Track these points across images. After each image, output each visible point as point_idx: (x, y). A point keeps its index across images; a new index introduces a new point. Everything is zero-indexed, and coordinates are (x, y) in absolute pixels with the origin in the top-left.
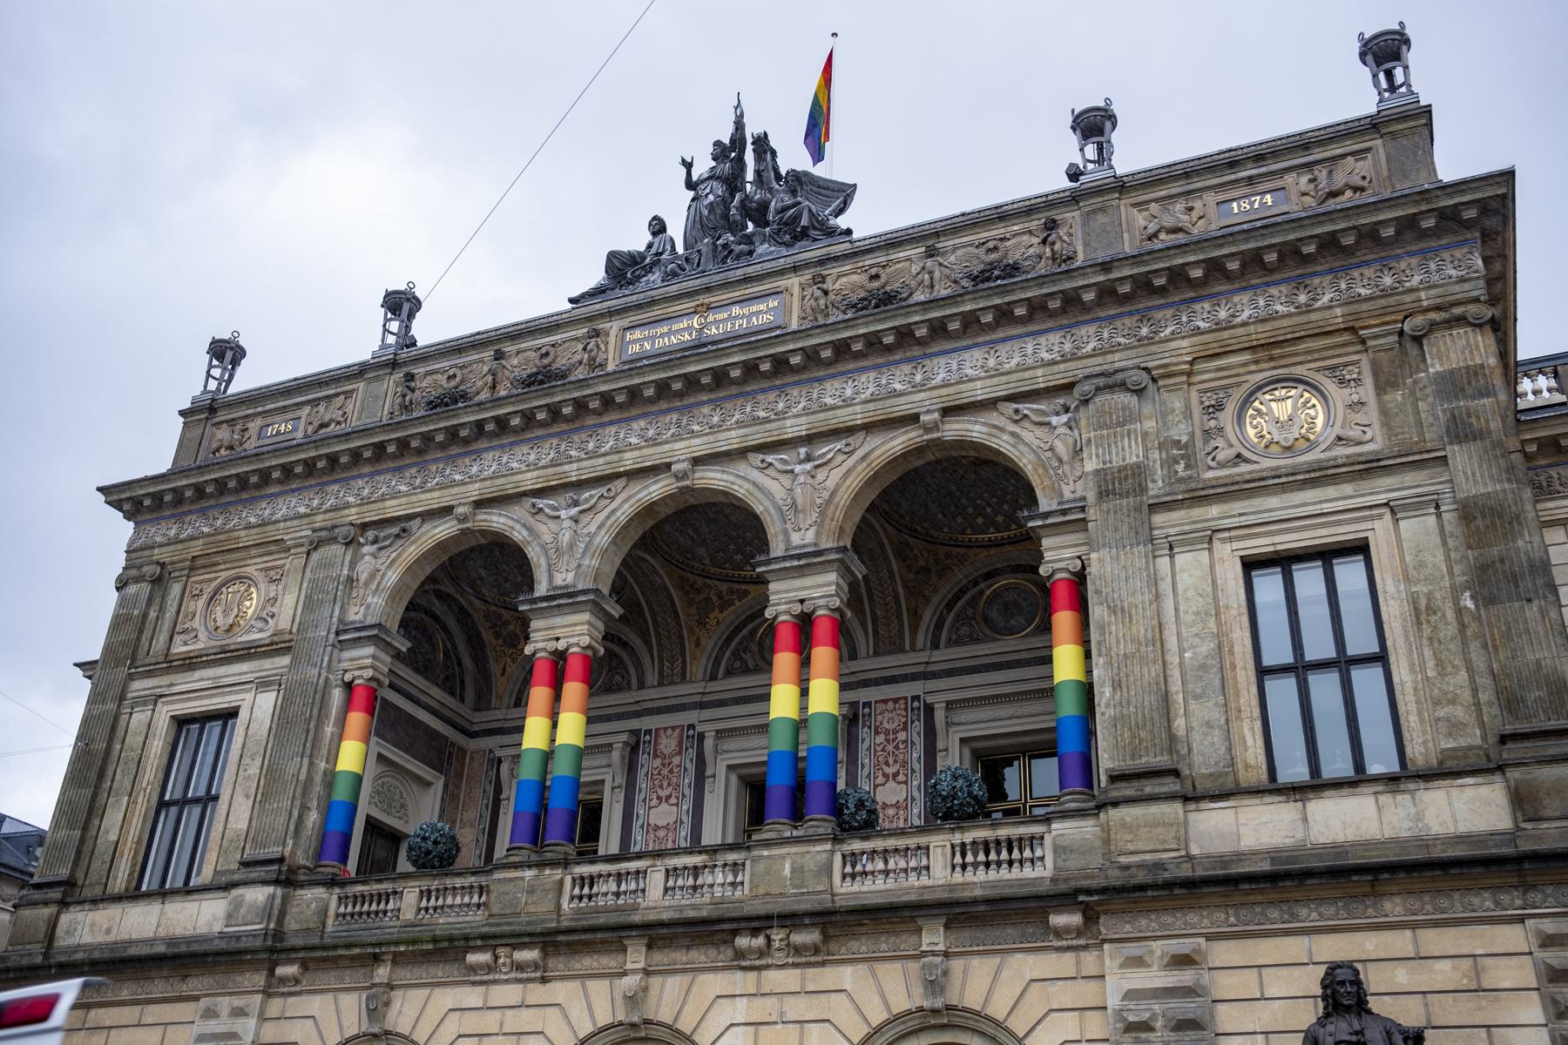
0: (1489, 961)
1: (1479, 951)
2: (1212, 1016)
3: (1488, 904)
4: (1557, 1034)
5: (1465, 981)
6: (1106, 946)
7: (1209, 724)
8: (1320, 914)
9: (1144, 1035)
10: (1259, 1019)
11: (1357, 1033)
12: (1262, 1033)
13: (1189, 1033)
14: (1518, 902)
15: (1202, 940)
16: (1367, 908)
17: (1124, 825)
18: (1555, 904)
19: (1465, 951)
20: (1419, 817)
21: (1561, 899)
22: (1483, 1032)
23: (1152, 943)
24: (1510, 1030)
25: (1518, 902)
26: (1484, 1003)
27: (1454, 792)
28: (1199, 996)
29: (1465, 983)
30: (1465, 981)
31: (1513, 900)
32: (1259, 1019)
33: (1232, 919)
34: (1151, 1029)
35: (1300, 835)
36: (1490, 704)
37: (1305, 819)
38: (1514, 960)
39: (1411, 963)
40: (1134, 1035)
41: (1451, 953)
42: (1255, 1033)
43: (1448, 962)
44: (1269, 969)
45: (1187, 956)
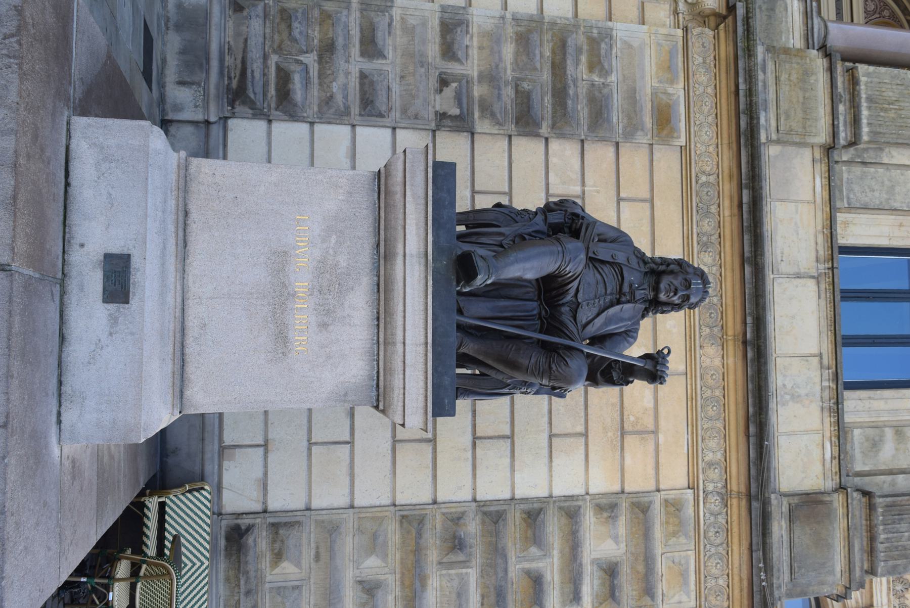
0: (651, 447)
2: (603, 140)
3: (709, 457)
4: (580, 503)
5: (632, 418)
6: (680, 32)
7: (891, 190)
9: (584, 58)
10: (598, 192)
11: (632, 293)
12: (583, 192)
13: (586, 111)
14: (710, 487)
15: (682, 141)
16: (711, 328)
17: (807, 73)
18: (708, 522)
19: (662, 423)
20: (795, 398)
22: (580, 428)
23: (681, 85)
24: (583, 457)
25: (710, 487)
26: (610, 434)
27: (818, 438)
28: (625, 128)
29: (630, 419)
30: (632, 418)
31: (712, 481)
32: (598, 192)
33: (704, 179)
34: (591, 69)
35: (784, 268)
36: (893, 484)
37: (798, 276)
38: (651, 472)
40: (585, 47)
41: (661, 409)
42: (583, 184)
43: (651, 405)
44: (648, 213)
45: (668, 121)
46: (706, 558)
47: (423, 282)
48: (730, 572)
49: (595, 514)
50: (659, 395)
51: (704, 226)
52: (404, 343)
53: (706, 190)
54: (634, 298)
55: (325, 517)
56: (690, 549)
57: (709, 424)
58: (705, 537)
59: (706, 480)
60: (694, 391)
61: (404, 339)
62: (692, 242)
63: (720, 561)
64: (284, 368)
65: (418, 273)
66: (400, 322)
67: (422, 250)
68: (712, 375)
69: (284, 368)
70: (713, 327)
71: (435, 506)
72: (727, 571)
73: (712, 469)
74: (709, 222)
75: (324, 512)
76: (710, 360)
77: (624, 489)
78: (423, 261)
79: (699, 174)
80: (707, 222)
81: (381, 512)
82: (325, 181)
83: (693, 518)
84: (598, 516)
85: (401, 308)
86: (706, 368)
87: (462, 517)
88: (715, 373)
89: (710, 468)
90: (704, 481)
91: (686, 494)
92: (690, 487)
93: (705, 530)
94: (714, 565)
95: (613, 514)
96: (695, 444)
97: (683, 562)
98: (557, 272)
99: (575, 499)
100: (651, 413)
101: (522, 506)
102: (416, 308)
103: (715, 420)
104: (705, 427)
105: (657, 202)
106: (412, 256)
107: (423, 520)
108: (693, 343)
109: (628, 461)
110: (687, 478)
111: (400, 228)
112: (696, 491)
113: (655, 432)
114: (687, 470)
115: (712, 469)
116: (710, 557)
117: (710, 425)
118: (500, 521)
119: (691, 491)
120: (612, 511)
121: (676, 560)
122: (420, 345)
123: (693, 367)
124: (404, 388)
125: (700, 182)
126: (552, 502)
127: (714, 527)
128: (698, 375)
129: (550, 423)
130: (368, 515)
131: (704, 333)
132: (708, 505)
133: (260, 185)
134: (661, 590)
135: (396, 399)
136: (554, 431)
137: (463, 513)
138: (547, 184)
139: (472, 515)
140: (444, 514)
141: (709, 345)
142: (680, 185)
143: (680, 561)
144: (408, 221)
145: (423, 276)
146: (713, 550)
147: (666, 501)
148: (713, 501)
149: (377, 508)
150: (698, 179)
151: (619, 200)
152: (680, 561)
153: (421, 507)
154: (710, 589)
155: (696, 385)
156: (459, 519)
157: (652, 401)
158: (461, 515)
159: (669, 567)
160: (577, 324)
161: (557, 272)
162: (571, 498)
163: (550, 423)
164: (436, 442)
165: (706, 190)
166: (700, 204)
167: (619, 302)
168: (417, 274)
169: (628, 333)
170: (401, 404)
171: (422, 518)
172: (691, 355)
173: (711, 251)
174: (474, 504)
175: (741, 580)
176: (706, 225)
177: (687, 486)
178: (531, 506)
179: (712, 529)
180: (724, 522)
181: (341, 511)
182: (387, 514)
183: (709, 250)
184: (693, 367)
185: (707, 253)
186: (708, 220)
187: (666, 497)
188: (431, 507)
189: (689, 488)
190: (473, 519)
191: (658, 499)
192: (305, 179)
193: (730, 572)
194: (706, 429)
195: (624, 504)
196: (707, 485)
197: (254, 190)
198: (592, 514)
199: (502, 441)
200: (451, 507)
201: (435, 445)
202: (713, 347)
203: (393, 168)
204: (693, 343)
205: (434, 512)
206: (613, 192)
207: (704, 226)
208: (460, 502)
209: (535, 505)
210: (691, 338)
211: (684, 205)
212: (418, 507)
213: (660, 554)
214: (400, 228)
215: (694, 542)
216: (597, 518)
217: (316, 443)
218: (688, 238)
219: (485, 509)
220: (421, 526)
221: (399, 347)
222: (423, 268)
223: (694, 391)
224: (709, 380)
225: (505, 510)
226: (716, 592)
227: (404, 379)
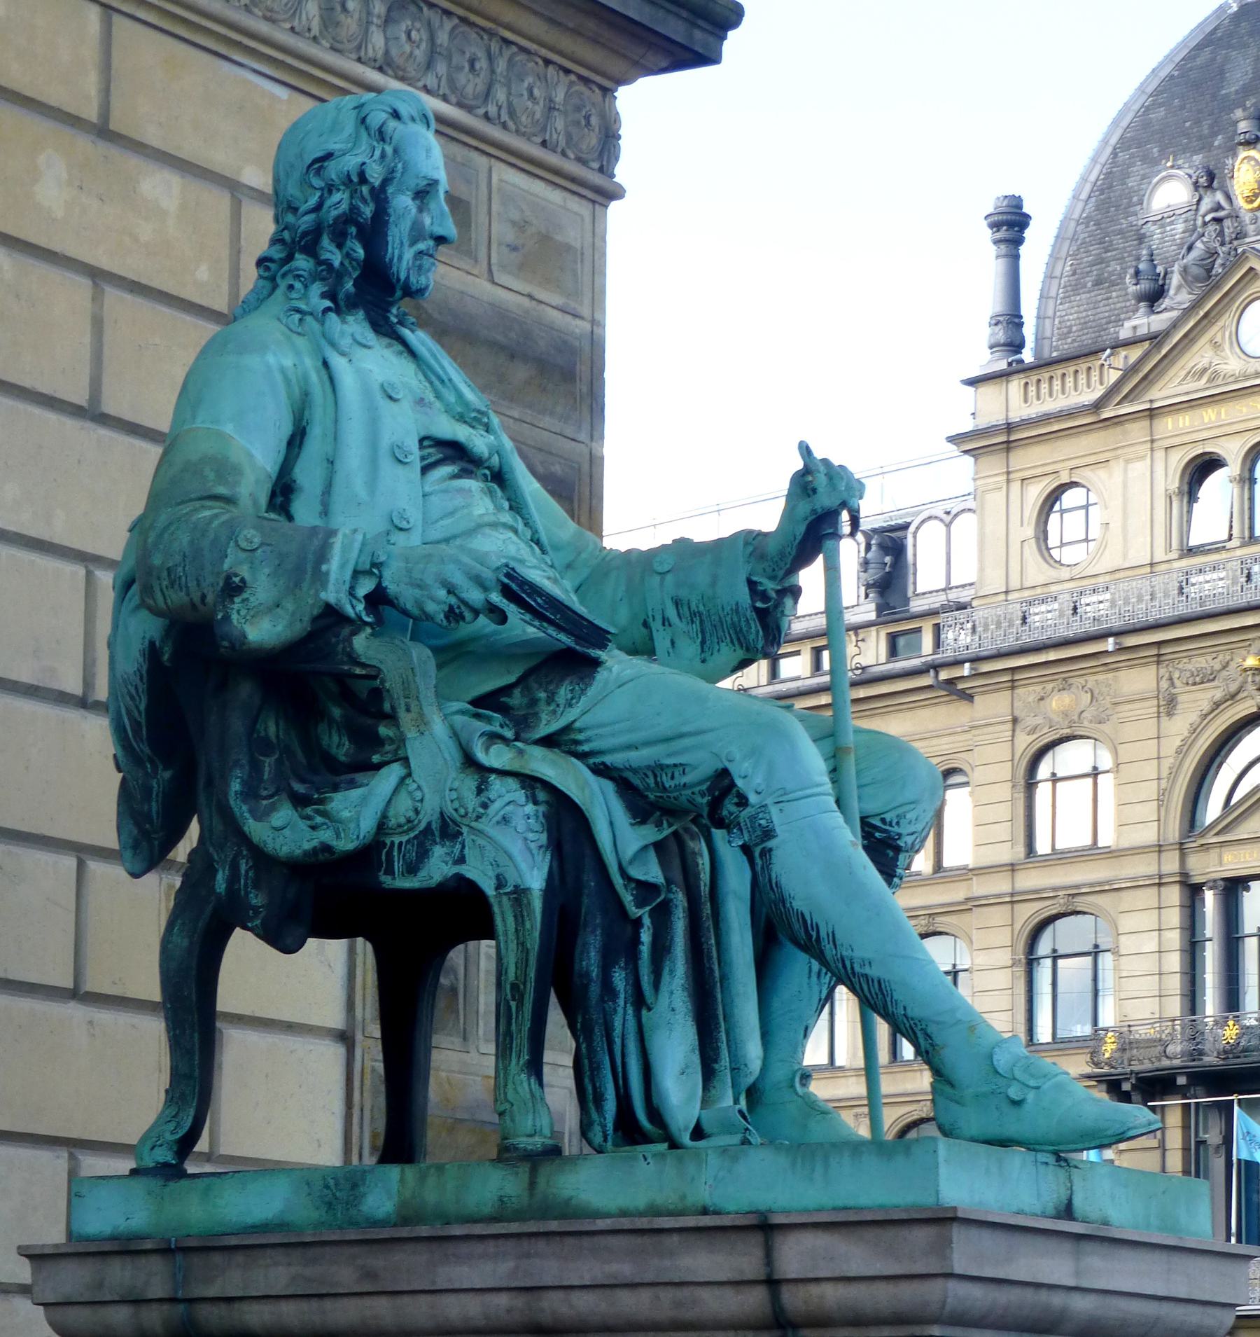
21: (462, 78)
46: (511, 124)
48: (544, 52)
56: (485, 170)
58: (469, 109)
59: (359, 48)
63: (526, 84)
66: (1136, 1307)
67: (1067, 1245)
72: (541, 62)
73: (342, 17)
89: (338, 24)
90: (359, 60)
93: (460, 105)
94: (529, 104)
96: (289, 60)
97: (515, 215)
115: (342, 17)
116: (512, 113)
121: (510, 236)
127: (460, 68)
132: (412, 72)
134: (555, 313)
143: (514, 223)
146: (500, 95)
148: (407, 48)
152: (514, 223)
154: (569, 137)
159: (521, 267)
175: (576, 32)
179: (462, 78)
180: (449, 24)
193: (544, 52)
196: (371, 53)
213: (488, 286)
215: (475, 155)
226: (578, 123)
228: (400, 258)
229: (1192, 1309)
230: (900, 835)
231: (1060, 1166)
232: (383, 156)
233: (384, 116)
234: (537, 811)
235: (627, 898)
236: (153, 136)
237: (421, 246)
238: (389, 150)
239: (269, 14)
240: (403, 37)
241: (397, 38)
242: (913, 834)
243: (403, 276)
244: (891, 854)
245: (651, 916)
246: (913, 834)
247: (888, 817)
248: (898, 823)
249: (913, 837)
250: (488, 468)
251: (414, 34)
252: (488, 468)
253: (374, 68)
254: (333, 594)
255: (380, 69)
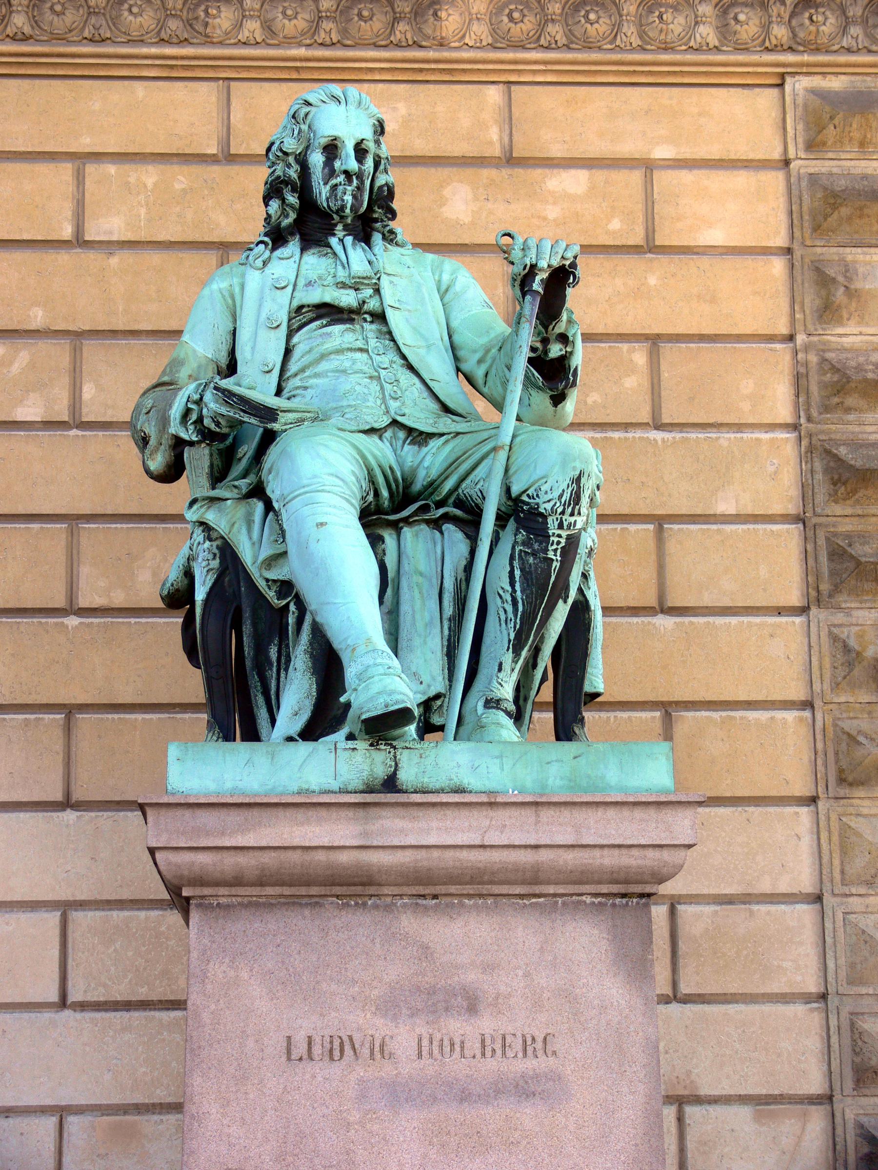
1: (662, 152)
8: (268, 27)
16: (396, 20)
19: (627, 148)
30: (615, 224)
31: (766, 28)
38: (741, 179)
39: (486, 173)
47: (414, 812)
49: (840, 322)
50: (559, 155)
51: (141, 26)
52: (537, 847)
53: (48, 16)
54: (369, 278)
55: (842, 961)
57: (630, 30)
60: (549, 67)
61: (526, 847)
62: (183, 58)
64: (583, 1078)
65: (397, 821)
66: (496, 856)
67: (350, 813)
68: (511, 19)
69: (583, 1078)
70: (395, 13)
71: (818, 703)
74: (130, 11)
75: (831, 964)
76: (475, 22)
77: (781, 248)
78: (373, 811)
79: (9, 31)
80: (131, 18)
81: (830, 832)
82: (213, 1007)
83: (853, 78)
84: (845, 315)
85: (464, 854)
86: (494, 32)
87: (844, 641)
88: (507, 11)
89: (735, 33)
91: (795, 94)
92: (779, 82)
95: (841, 279)
98: (354, 501)
99: (802, 370)
100: (601, 175)
101: (820, 498)
102: (467, 824)
103: (621, 16)
104: (636, 41)
105: (86, 143)
106: (365, 834)
107: (849, 734)
108: (433, 66)
109: (715, 237)
110: (757, 90)
111: (308, 857)
112: (789, 70)
113: (649, 166)
114: (739, 90)
115: (738, 27)
117: (633, 29)
118: (853, 553)
119: (789, 80)
120: (834, 280)
122: (538, 816)
123: (491, 67)
124: (619, 846)
125: (27, 30)
126: (810, 425)
128: (510, 55)
129: (626, 426)
130: (836, 862)
131: (409, 36)
133: (229, 1136)
135: (640, 862)
136: (644, 415)
137: (834, 639)
138: (48, 425)
139: (839, 618)
140: (836, 686)
141: (438, 23)
142: (37, 82)
144: (296, 842)
145: (401, 811)
147: (810, 146)
149: (822, 841)
150: (20, 36)
151: (79, 242)
153: (819, 737)
155: (536, 62)
156: (846, 649)
157: (573, 172)
158: (840, 645)
160: (442, 435)
161: (354, 501)
162: (799, 381)
163: (626, 426)
164: (670, 703)
165: (48, 16)
166: (86, 34)
167: (380, 317)
168: (399, 823)
169: (443, 288)
170: (651, 853)
171: (845, 737)
172: (464, 71)
173: (206, 12)
174: (814, 611)
176: (139, 19)
177: (775, 92)
178: (819, 476)
181: (828, 925)
182: (834, 817)
183: (202, 14)
184: (491, 67)
185: (210, 21)
186: (126, 13)
187: (801, 146)
188: (819, 716)
189: (781, 85)
190: (849, 615)
191: (802, 166)
192: (211, 1045)
194: (641, 38)
195: (819, 250)
196: (774, 42)
197: (237, 1147)
198: (840, 330)
199: (672, 546)
200: (821, 669)
201: (677, 703)
202: (443, 14)
203: (186, 873)
204: (433, 66)
205: (831, 706)
206: (64, 258)
207: (141, 26)
208: (810, 646)
209: (818, 465)
210: (421, 70)
211: (86, 73)
212: (820, 746)
214: (308, 857)
216: (848, 319)
217: (675, 984)
218: (172, 67)
219: (825, 587)
220: (861, 739)
221: (544, 856)
222: (385, 812)
223: (549, 67)
224: (524, 27)
225: (828, 539)
227: (602, 847)
228: (320, 193)
229: (597, 853)
230: (538, 504)
231: (379, 749)
232: (300, 131)
233: (297, 106)
234: (212, 546)
235: (271, 595)
236: (557, 151)
237: (334, 181)
238: (304, 127)
239: (664, 46)
240: (807, 22)
241: (802, 25)
242: (549, 501)
243: (325, 205)
244: (540, 520)
245: (295, 604)
246: (549, 501)
247: (530, 492)
248: (537, 496)
249: (552, 503)
250: (366, 313)
251: (814, 18)
252: (366, 313)
253: (784, 50)
254: (175, 428)
255: (791, 49)
